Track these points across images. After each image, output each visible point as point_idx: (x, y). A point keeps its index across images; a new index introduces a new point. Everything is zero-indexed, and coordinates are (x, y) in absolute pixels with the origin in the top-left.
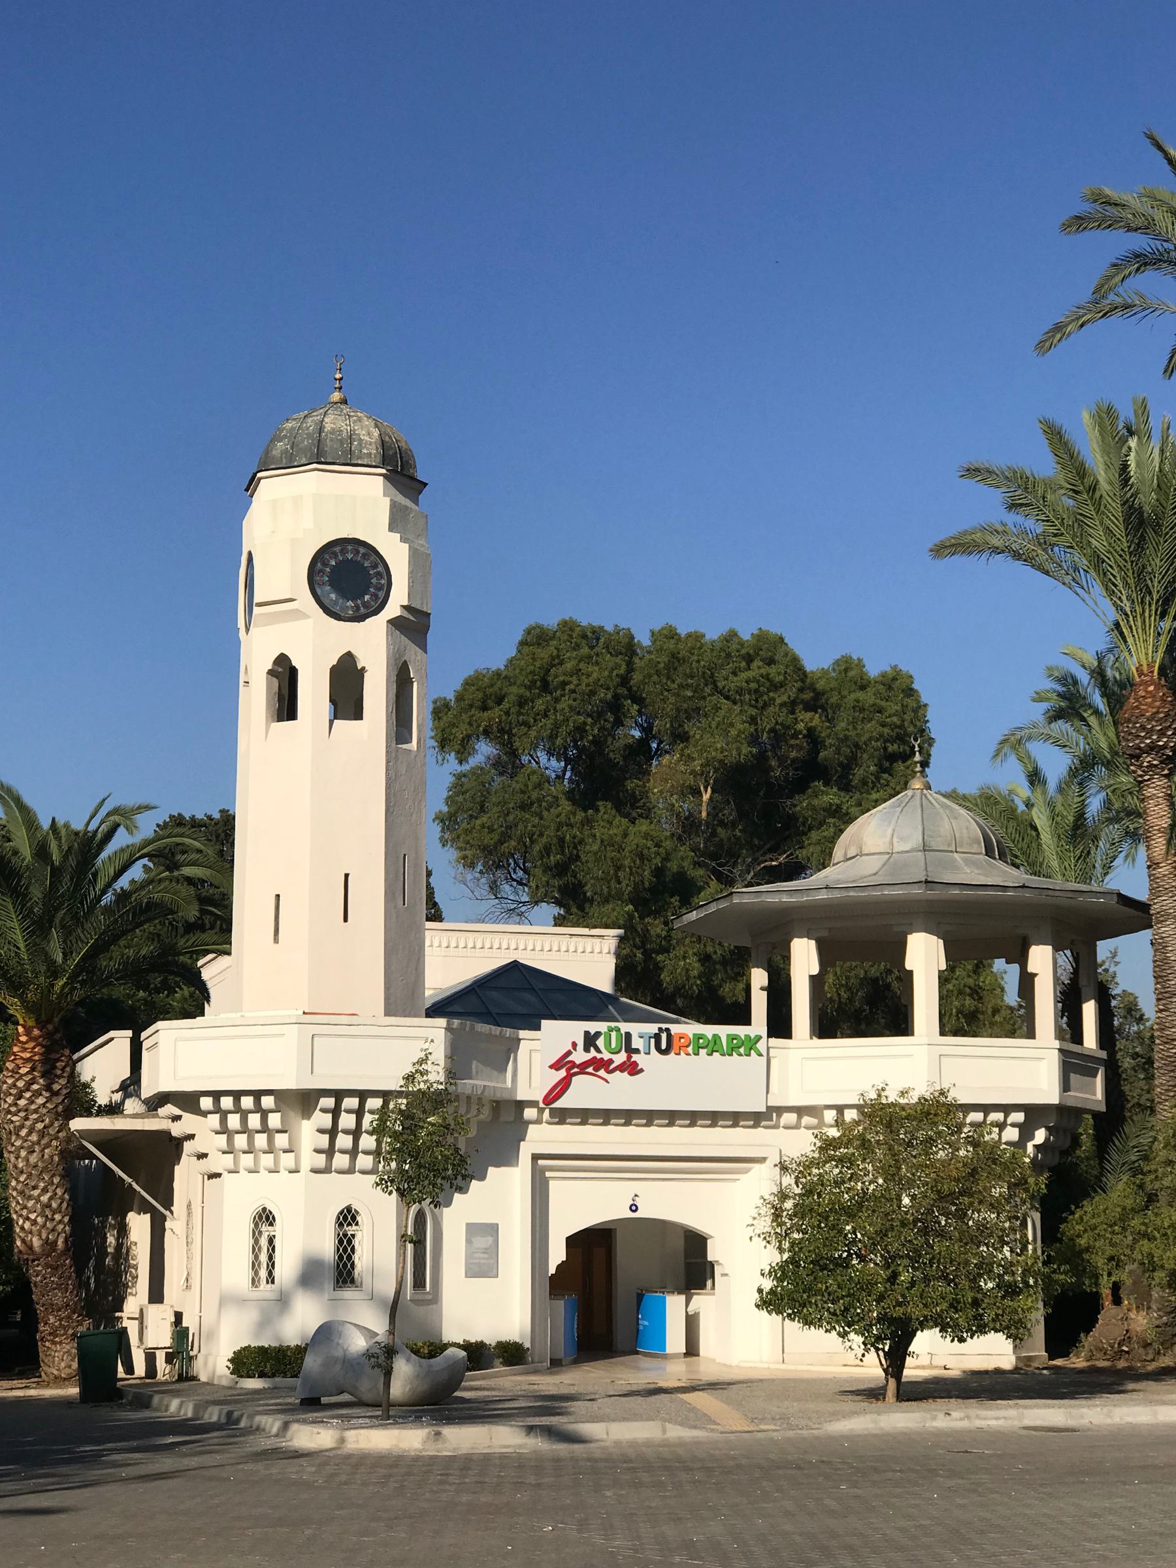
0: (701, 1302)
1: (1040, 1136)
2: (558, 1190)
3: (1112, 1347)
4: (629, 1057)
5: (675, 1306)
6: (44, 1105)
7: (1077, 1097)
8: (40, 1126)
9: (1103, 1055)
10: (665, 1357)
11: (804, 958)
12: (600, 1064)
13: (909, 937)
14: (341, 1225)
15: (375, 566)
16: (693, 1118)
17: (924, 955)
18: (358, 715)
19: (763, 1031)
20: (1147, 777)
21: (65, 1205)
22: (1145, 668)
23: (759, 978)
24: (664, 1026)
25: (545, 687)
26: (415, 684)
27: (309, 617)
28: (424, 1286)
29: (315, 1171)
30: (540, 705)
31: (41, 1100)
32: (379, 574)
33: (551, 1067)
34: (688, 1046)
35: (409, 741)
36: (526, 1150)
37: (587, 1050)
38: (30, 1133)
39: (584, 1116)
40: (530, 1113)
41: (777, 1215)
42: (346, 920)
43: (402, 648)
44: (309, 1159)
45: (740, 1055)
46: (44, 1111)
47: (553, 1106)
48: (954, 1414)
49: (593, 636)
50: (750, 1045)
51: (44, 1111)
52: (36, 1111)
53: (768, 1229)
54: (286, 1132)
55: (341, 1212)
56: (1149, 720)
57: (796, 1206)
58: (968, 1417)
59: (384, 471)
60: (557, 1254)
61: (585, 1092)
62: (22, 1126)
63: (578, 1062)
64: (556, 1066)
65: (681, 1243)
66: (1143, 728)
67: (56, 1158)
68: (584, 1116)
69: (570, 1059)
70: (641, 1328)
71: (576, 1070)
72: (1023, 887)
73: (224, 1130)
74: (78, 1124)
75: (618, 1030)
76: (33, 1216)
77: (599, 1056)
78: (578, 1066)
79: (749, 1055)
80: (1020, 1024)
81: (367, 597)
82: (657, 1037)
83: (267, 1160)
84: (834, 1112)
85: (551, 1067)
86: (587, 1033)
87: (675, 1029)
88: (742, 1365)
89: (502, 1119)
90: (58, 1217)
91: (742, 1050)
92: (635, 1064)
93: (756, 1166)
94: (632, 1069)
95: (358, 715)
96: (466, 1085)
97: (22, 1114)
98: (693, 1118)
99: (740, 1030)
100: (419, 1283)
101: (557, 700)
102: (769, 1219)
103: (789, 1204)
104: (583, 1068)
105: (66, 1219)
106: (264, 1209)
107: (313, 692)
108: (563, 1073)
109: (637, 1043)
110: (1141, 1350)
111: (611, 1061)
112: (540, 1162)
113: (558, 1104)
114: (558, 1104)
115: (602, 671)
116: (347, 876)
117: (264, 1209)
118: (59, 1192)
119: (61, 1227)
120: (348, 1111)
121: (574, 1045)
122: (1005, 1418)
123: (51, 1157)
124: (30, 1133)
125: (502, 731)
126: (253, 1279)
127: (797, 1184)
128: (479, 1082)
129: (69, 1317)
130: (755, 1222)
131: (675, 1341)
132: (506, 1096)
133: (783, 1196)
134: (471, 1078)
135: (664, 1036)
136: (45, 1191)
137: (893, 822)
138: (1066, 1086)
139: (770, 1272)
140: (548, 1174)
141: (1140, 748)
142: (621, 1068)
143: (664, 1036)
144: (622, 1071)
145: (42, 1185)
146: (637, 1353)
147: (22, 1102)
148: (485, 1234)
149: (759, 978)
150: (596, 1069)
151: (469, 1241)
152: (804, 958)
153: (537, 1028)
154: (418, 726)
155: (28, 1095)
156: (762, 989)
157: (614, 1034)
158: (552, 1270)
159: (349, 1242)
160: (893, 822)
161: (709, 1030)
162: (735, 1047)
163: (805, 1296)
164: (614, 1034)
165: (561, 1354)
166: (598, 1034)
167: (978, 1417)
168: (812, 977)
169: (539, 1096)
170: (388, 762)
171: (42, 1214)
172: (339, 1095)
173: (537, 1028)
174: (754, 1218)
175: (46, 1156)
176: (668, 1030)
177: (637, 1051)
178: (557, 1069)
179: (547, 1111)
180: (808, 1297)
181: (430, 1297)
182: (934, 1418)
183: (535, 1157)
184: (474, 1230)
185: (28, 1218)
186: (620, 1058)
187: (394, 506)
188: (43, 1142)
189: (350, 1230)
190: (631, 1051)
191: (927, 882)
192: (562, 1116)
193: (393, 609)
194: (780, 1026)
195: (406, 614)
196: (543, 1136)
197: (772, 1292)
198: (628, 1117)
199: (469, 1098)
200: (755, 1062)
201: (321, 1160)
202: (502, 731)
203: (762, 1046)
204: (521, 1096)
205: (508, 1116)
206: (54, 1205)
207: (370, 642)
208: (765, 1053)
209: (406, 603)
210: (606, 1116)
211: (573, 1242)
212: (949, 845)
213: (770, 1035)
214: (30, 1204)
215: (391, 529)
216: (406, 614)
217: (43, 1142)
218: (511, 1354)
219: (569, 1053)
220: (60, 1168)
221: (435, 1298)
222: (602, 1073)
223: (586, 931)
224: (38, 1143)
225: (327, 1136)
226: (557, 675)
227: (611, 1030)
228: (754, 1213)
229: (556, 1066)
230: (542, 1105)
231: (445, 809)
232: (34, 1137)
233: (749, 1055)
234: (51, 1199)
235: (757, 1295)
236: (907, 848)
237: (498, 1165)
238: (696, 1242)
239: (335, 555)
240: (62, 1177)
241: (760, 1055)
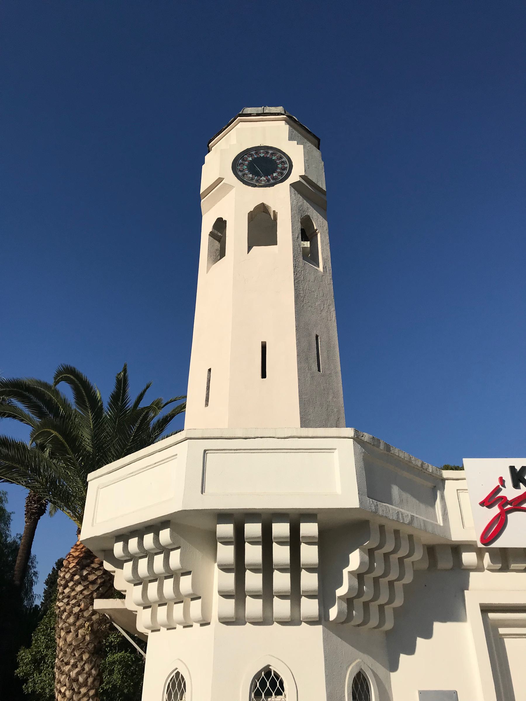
6: (81, 592)
8: (76, 610)
18: (272, 240)
21: (90, 680)
26: (319, 235)
27: (233, 187)
29: (226, 622)
31: (79, 588)
32: (283, 163)
33: (482, 504)
36: (473, 599)
37: (516, 486)
38: (68, 617)
40: (469, 558)
42: (264, 375)
46: (81, 597)
51: (81, 597)
52: (75, 597)
54: (189, 573)
55: (257, 676)
62: (65, 610)
63: (509, 499)
64: (487, 503)
67: (88, 638)
69: (500, 494)
71: (509, 506)
73: (137, 581)
74: (99, 604)
76: (63, 690)
78: (510, 503)
81: (275, 175)
85: (482, 504)
86: (512, 469)
90: (83, 690)
95: (272, 240)
97: (66, 600)
104: (517, 505)
105: (92, 693)
106: (178, 674)
107: (237, 234)
108: (496, 510)
112: (491, 615)
113: (498, 544)
114: (498, 544)
118: (87, 668)
123: (84, 637)
124: (68, 617)
134: (392, 504)
136: (75, 666)
140: (502, 631)
145: (72, 661)
147: (67, 590)
154: (323, 258)
155: (71, 584)
169: (474, 535)
171: (72, 689)
172: (239, 518)
175: (80, 636)
178: (490, 506)
179: (487, 556)
183: (486, 609)
185: (60, 692)
188: (78, 624)
192: (506, 560)
193: (295, 177)
196: (486, 586)
201: (229, 607)
204: (457, 535)
205: (445, 563)
206: (81, 679)
207: (279, 199)
209: (303, 174)
214: (63, 678)
217: (78, 624)
219: (497, 490)
220: (91, 646)
224: (74, 624)
225: (231, 577)
229: (487, 503)
230: (480, 545)
232: (71, 620)
234: (78, 674)
237: (444, 619)
239: (252, 155)
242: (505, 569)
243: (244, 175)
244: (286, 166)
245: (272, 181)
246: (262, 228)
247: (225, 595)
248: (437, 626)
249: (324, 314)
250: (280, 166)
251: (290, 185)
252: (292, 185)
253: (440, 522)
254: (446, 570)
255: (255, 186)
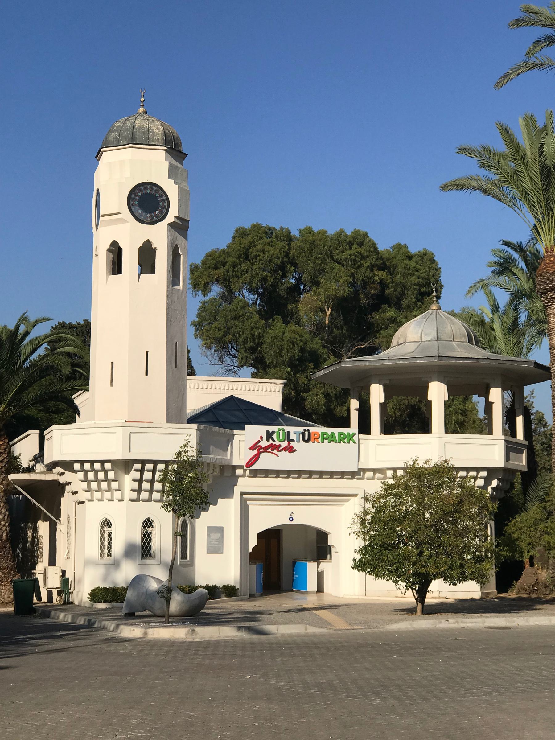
0: (324, 566)
1: (495, 483)
2: (252, 510)
3: (529, 588)
4: (289, 444)
5: (311, 568)
7: (514, 464)
9: (526, 443)
10: (307, 593)
11: (377, 394)
12: (274, 447)
13: (430, 383)
14: (144, 527)
15: (161, 196)
16: (321, 474)
17: (437, 393)
18: (153, 271)
19: (356, 431)
20: (549, 304)
21: (6, 517)
22: (549, 249)
23: (354, 404)
24: (306, 428)
25: (247, 257)
26: (182, 256)
28: (186, 558)
29: (132, 500)
30: (244, 267)
32: (163, 201)
33: (250, 449)
34: (318, 438)
35: (179, 285)
36: (237, 490)
37: (268, 440)
39: (266, 473)
40: (239, 472)
41: (363, 522)
42: (147, 375)
43: (175, 238)
44: (129, 494)
45: (345, 443)
47: (252, 468)
48: (450, 621)
49: (269, 232)
50: (349, 438)
53: (358, 529)
54: (117, 481)
55: (145, 521)
56: (551, 275)
57: (372, 518)
58: (457, 622)
59: (166, 148)
60: (253, 542)
61: (267, 461)
63: (263, 446)
64: (252, 448)
65: (314, 537)
66: (548, 279)
68: (266, 473)
69: (259, 444)
70: (295, 578)
71: (262, 450)
72: (487, 359)
73: (86, 480)
74: (13, 477)
75: (283, 430)
77: (274, 443)
78: (263, 448)
79: (349, 443)
80: (485, 428)
81: (157, 212)
82: (303, 434)
83: (107, 495)
84: (392, 471)
85: (250, 449)
86: (268, 432)
87: (312, 430)
88: (345, 597)
89: (226, 474)
91: (346, 440)
92: (292, 447)
93: (352, 499)
94: (290, 449)
95: (153, 271)
96: (207, 458)
98: (321, 474)
99: (345, 430)
100: (184, 556)
101: (253, 264)
102: (359, 525)
103: (369, 517)
104: (266, 449)
105: (7, 524)
106: (106, 519)
107: (130, 260)
108: (256, 452)
109: (293, 437)
110: (544, 589)
111: (280, 446)
112: (245, 496)
113: (254, 467)
114: (254, 467)
115: (276, 250)
116: (147, 352)
117: (106, 519)
119: (5, 528)
120: (148, 471)
121: (261, 438)
122: (475, 622)
125: (225, 280)
126: (101, 554)
127: (373, 507)
128: (214, 456)
129: (9, 573)
130: (352, 526)
131: (312, 585)
132: (227, 463)
133: (366, 513)
135: (307, 433)
137: (422, 325)
138: (507, 459)
139: (359, 551)
140: (248, 502)
141: (546, 289)
142: (285, 449)
143: (307, 433)
144: (285, 451)
146: (293, 591)
148: (216, 532)
149: (354, 404)
150: (273, 450)
151: (208, 535)
152: (377, 394)
153: (243, 429)
156: (356, 410)
157: (281, 432)
158: (250, 550)
159: (149, 536)
160: (422, 325)
161: (329, 430)
162: (342, 438)
163: (377, 563)
164: (281, 432)
165: (254, 591)
166: (273, 432)
167: (462, 622)
168: (380, 404)
169: (243, 463)
170: (168, 295)
172: (143, 462)
173: (243, 429)
174: (352, 524)
176: (308, 430)
177: (293, 441)
178: (253, 450)
179: (248, 471)
180: (378, 563)
181: (189, 563)
182: (440, 623)
183: (242, 494)
184: (211, 530)
186: (285, 444)
187: (171, 165)
189: (149, 530)
190: (290, 441)
191: (439, 356)
192: (255, 473)
193: (170, 218)
194: (365, 428)
195: (177, 221)
196: (245, 483)
197: (360, 560)
198: (288, 474)
199: (208, 464)
200: (352, 447)
201: (134, 495)
202: (225, 280)
203: (355, 438)
204: (235, 463)
205: (228, 473)
207: (159, 235)
208: (357, 442)
209: (177, 215)
210: (277, 473)
211: (261, 536)
212: (450, 338)
213: (359, 433)
215: (169, 178)
216: (177, 221)
218: (230, 591)
219: (259, 442)
220: (4, 499)
221: (192, 563)
222: (275, 451)
223: (267, 380)
226: (253, 252)
227: (280, 430)
228: (352, 522)
229: (252, 448)
230: (245, 468)
231: (197, 319)
233: (349, 443)
235: (353, 562)
236: (429, 339)
237: (223, 497)
238: (322, 536)
239: (141, 191)
240: (5, 503)
241: (355, 443)
242: (255, 476)
243: (134, 199)
244: (165, 204)
245: (155, 219)
246: (147, 259)
247: (133, 490)
248: (220, 500)
249: (181, 323)
250: (161, 204)
251: (168, 224)
252: (170, 225)
253: (229, 457)
254: (227, 476)
255: (142, 222)
